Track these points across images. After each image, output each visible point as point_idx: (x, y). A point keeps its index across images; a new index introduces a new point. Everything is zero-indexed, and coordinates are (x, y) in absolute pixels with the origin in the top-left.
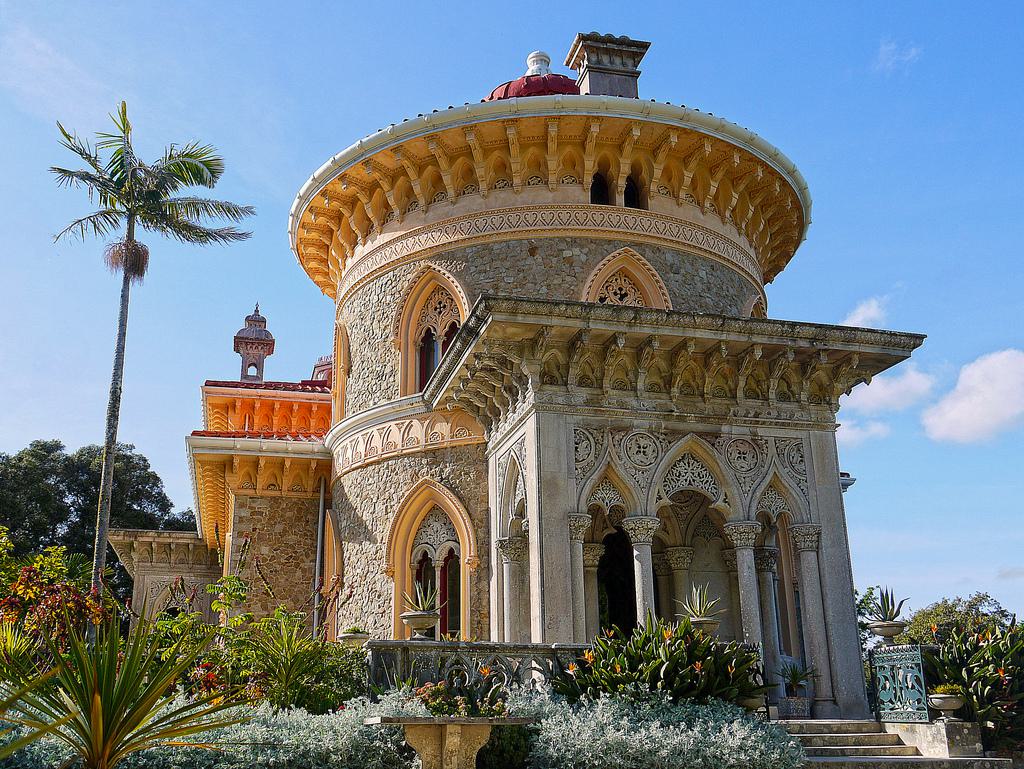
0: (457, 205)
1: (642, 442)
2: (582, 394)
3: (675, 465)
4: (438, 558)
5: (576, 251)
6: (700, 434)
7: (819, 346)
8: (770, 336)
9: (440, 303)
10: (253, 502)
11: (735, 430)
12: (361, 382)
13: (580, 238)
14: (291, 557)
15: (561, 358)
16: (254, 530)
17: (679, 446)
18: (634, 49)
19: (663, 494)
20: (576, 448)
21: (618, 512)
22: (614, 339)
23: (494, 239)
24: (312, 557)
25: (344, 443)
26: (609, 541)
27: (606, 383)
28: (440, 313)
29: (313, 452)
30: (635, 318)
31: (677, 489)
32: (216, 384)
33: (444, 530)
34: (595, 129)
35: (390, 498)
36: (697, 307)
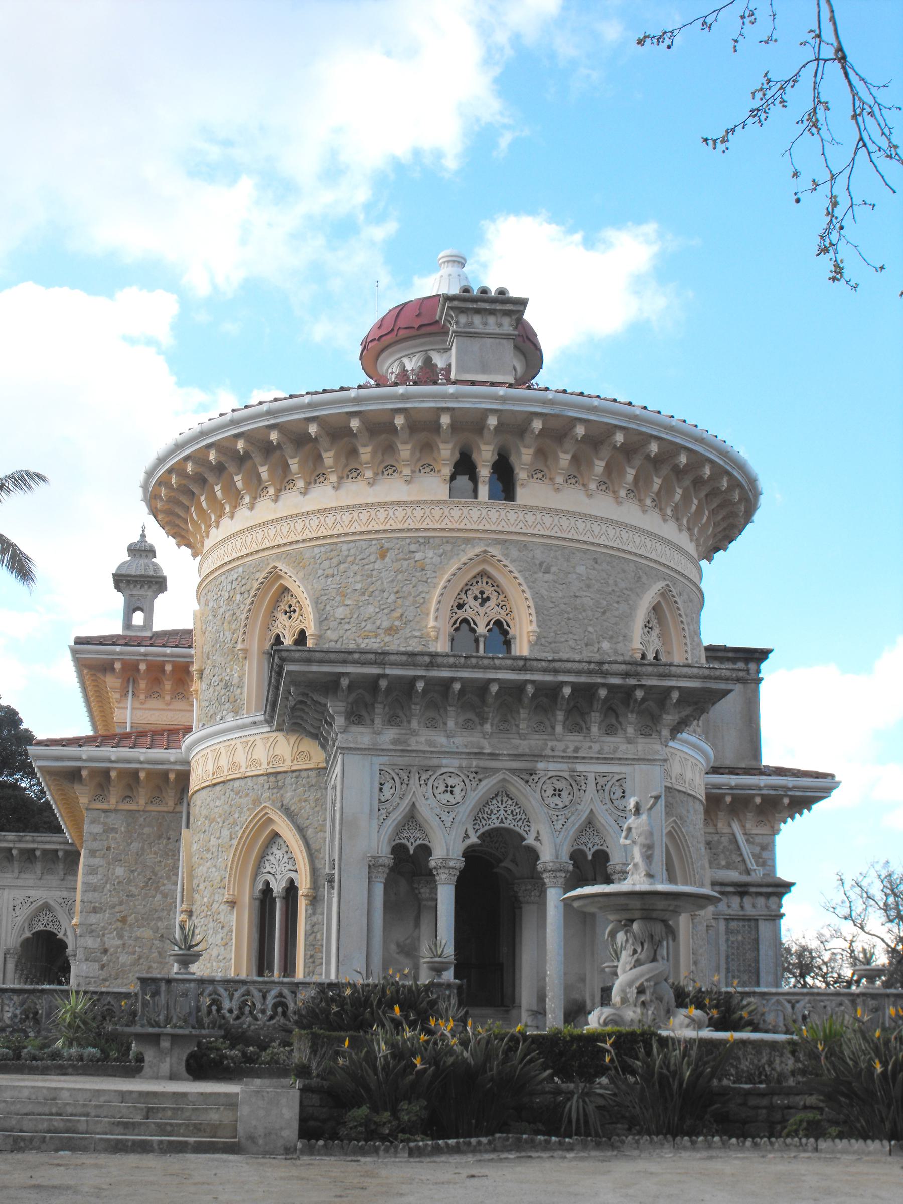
0: (307, 497)
1: (451, 782)
2: (389, 735)
3: (487, 803)
4: (278, 887)
5: (430, 554)
6: (513, 771)
7: (632, 682)
8: (579, 672)
9: (290, 606)
10: (107, 817)
11: (551, 766)
12: (211, 690)
13: (434, 537)
14: (150, 879)
16: (108, 849)
17: (488, 784)
19: (471, 833)
20: (381, 789)
21: (425, 851)
23: (342, 539)
24: (174, 878)
25: (205, 752)
29: (169, 762)
30: (431, 662)
31: (486, 828)
33: (286, 859)
35: (235, 823)
36: (569, 609)
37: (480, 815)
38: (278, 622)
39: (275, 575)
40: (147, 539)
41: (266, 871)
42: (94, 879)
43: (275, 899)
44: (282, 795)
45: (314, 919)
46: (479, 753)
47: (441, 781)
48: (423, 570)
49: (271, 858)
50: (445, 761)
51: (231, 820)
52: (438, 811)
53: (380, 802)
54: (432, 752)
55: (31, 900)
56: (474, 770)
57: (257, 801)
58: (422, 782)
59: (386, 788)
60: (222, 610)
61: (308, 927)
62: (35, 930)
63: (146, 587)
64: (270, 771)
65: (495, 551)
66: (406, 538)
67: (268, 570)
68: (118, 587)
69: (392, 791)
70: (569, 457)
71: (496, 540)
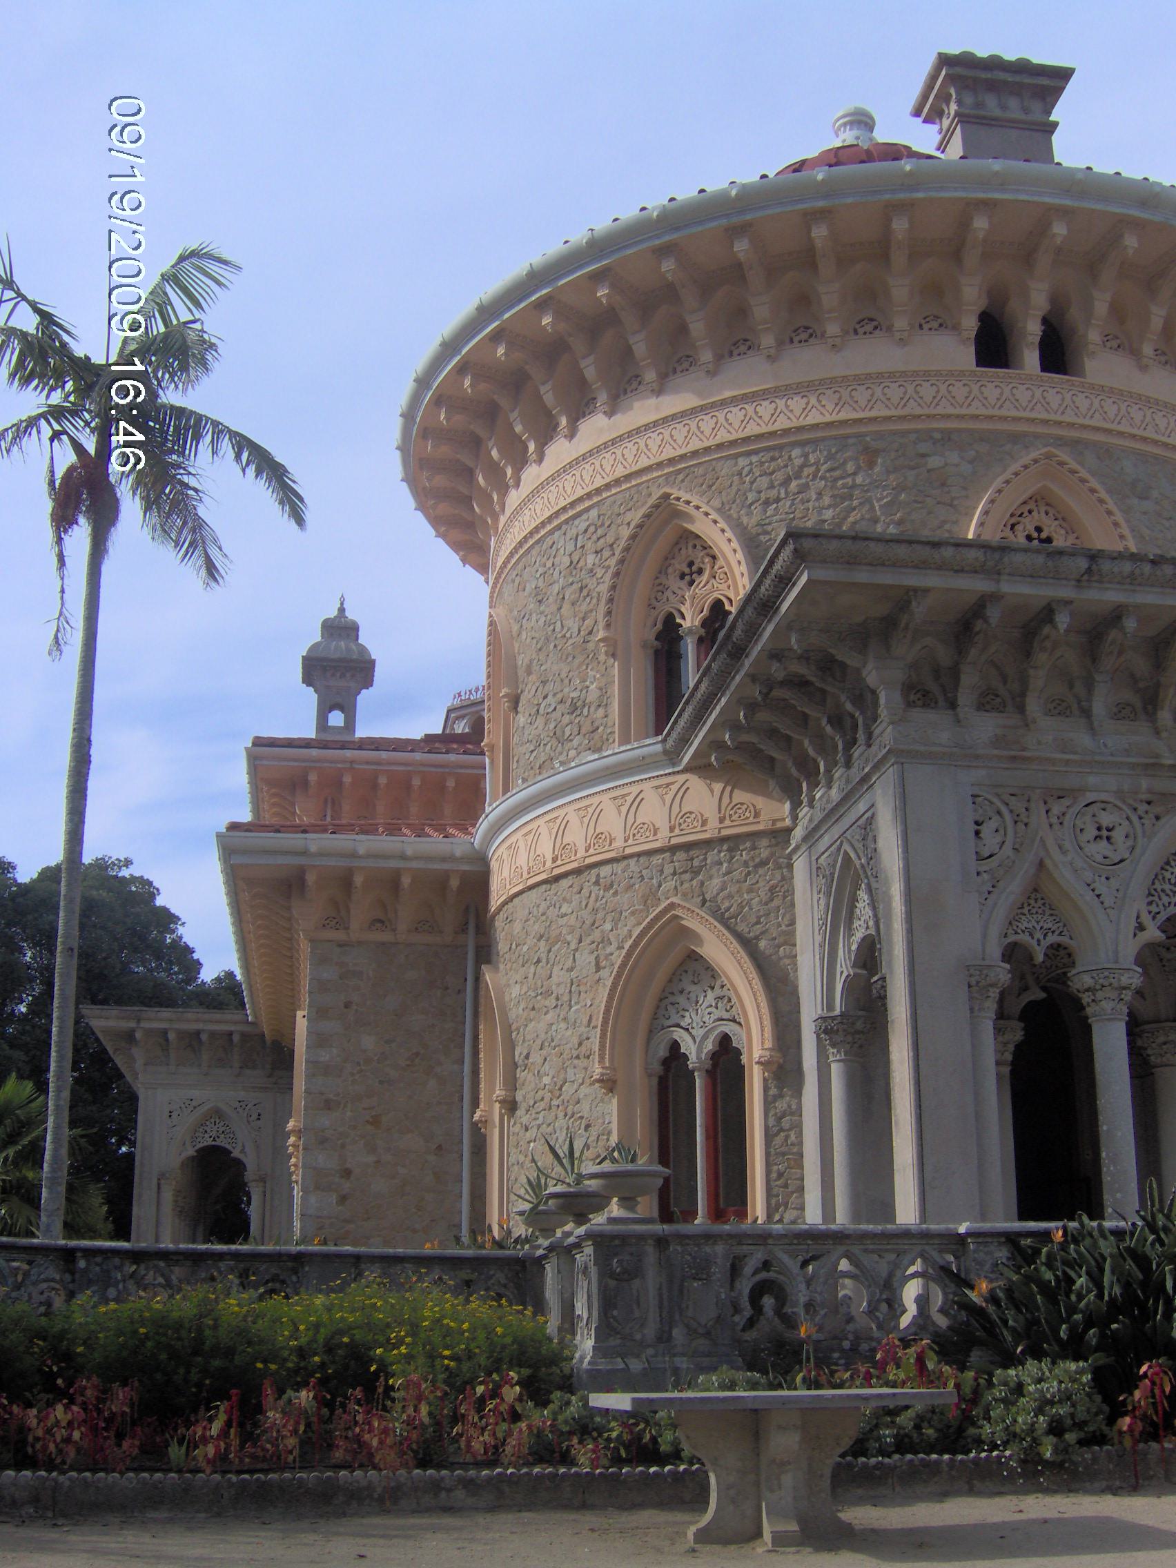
1: (1106, 819)
2: (984, 727)
3: (1168, 863)
4: (695, 1050)
5: (954, 457)
9: (691, 564)
12: (540, 721)
14: (417, 1054)
15: (944, 655)
18: (1045, 81)
20: (977, 833)
21: (1061, 955)
22: (1047, 613)
25: (513, 839)
26: (1030, 1014)
27: (1033, 706)
28: (691, 583)
29: (451, 858)
30: (1089, 571)
32: (272, 743)
34: (980, 223)
35: (605, 941)
37: (1158, 886)
38: (668, 593)
39: (665, 511)
40: (347, 614)
41: (670, 1022)
42: (324, 1056)
43: (693, 1072)
44: (702, 884)
45: (781, 1105)
46: (1153, 765)
47: (1088, 818)
48: (943, 485)
49: (681, 1000)
50: (1092, 780)
51: (597, 935)
52: (1088, 875)
53: (980, 858)
54: (1067, 762)
55: (194, 1103)
56: (1144, 797)
57: (650, 897)
58: (1054, 820)
59: (986, 830)
60: (556, 588)
61: (771, 1122)
62: (201, 1145)
63: (348, 675)
64: (674, 841)
65: (1063, 455)
66: (909, 432)
67: (651, 501)
68: (308, 679)
69: (999, 839)
70: (1163, 313)
71: (1060, 438)
